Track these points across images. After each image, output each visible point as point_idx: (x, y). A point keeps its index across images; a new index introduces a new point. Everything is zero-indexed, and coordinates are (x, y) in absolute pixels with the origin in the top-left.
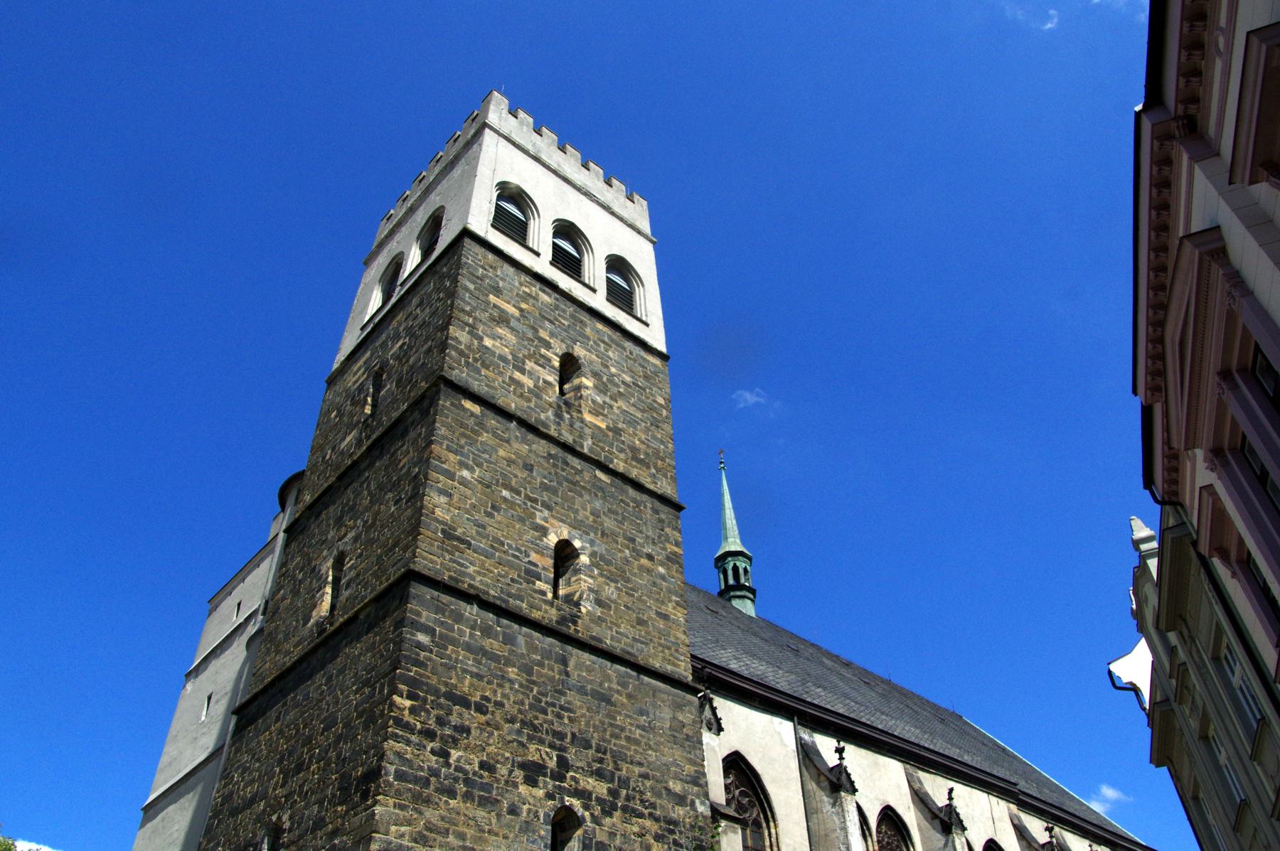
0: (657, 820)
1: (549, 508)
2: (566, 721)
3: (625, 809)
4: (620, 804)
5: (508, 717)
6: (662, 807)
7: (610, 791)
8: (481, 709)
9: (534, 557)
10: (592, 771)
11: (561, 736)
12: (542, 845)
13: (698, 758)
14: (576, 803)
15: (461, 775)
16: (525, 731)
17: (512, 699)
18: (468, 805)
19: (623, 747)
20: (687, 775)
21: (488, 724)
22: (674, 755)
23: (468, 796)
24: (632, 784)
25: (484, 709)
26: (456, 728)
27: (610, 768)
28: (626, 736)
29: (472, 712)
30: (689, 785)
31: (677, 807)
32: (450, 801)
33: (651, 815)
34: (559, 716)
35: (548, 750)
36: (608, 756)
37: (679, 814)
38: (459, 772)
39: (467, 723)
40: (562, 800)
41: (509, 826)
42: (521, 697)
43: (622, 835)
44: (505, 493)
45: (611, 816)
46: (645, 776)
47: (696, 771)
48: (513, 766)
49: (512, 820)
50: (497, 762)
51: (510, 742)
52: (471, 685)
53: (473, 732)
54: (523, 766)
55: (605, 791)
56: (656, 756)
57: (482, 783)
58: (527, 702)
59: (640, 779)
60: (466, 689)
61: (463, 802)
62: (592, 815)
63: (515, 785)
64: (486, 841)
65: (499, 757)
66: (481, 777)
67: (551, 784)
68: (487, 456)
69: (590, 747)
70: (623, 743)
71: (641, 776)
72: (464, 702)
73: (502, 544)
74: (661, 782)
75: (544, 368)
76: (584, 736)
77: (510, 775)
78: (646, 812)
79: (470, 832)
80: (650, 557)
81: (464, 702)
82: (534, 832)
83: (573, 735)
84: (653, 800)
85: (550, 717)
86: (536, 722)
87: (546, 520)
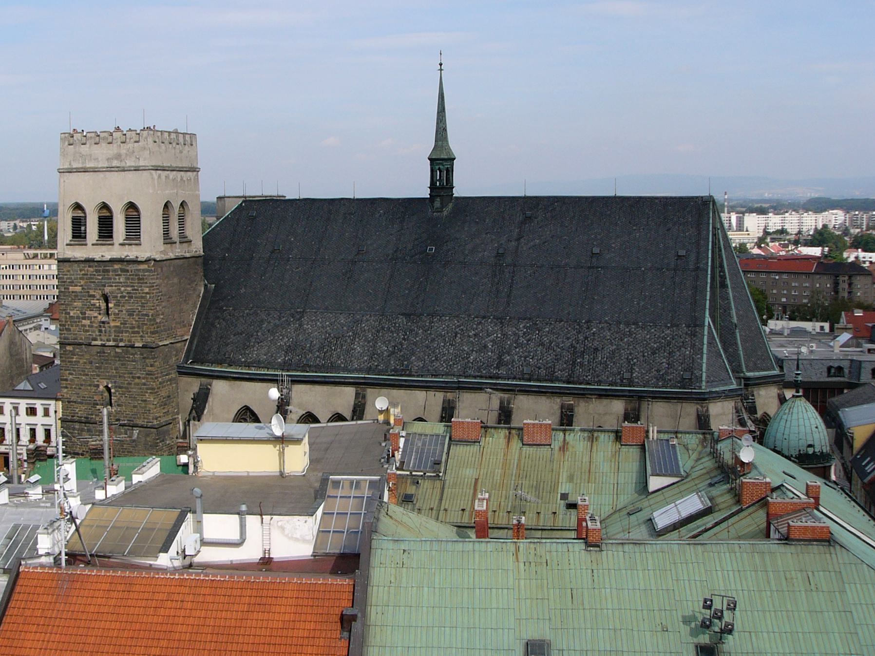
1: (98, 375)
9: (96, 398)
44: (84, 378)
68: (76, 366)
73: (85, 397)
75: (93, 310)
80: (139, 378)
87: (98, 381)
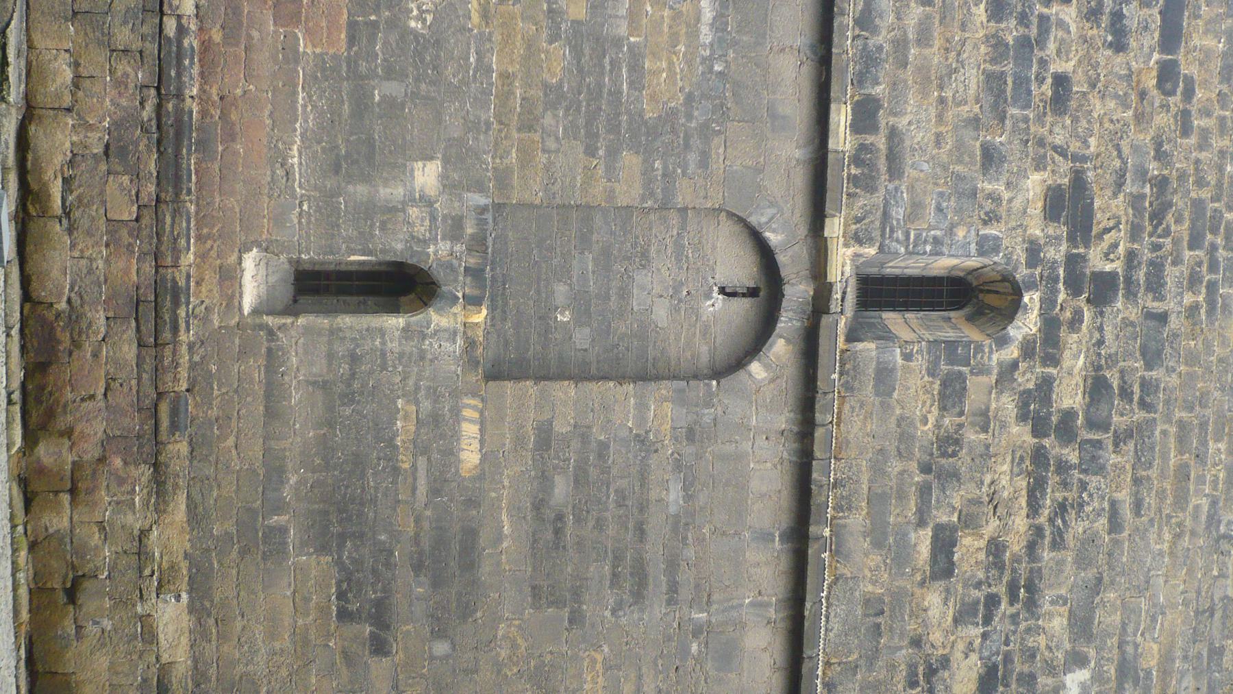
0: (1032, 547)
2: (1188, 299)
3: (1039, 456)
4: (1047, 442)
5: (1166, 147)
6: (1061, 563)
7: (1069, 415)
8: (1167, 74)
10: (1098, 368)
11: (1156, 286)
12: (938, 233)
13: (1179, 682)
14: (1027, 324)
15: (1034, 32)
16: (1147, 190)
17: (1203, 155)
18: (983, 49)
19: (1165, 457)
20: (1136, 646)
21: (1143, 95)
22: (1174, 606)
23: (998, 46)
24: (1094, 481)
25: (1169, 86)
26: (1117, 16)
27: (1116, 419)
28: (1187, 465)
29: (1156, 56)
30: (1116, 651)
31: (1064, 610)
32: (982, 6)
33: (1039, 531)
34: (1194, 281)
35: (1121, 249)
36: (1140, 415)
37: (1051, 615)
38: (1040, 26)
39: (1133, 44)
40: (1032, 286)
41: (960, 146)
42: (1211, 178)
43: (987, 447)
45: (1023, 417)
46: (1115, 524)
47: (1148, 673)
48: (1075, 158)
49: (972, 155)
50: (1075, 120)
51: (1118, 148)
52: (1208, 53)
53: (1120, 59)
54: (1078, 180)
55: (1067, 403)
56: (1161, 554)
57: (1028, 80)
58: (1205, 194)
59: (1106, 505)
60: (1196, 41)
61: (986, 36)
62: (1014, 365)
63: (1039, 165)
64: (925, 94)
65: (1084, 123)
66: (1041, 80)
67: (1057, 253)
69: (1149, 366)
70: (1172, 462)
71: (1113, 503)
72: (1171, 37)
74: (1111, 568)
76: (1168, 350)
77: (1055, 148)
78: (1042, 519)
79: (934, 54)
81: (1171, 37)
82: (959, 211)
83: (1163, 318)
84: (1069, 537)
85: (1187, 254)
86: (1170, 218)
